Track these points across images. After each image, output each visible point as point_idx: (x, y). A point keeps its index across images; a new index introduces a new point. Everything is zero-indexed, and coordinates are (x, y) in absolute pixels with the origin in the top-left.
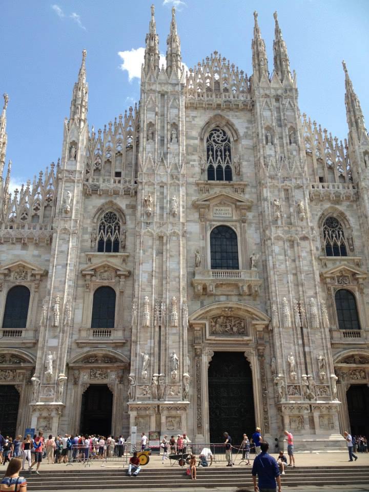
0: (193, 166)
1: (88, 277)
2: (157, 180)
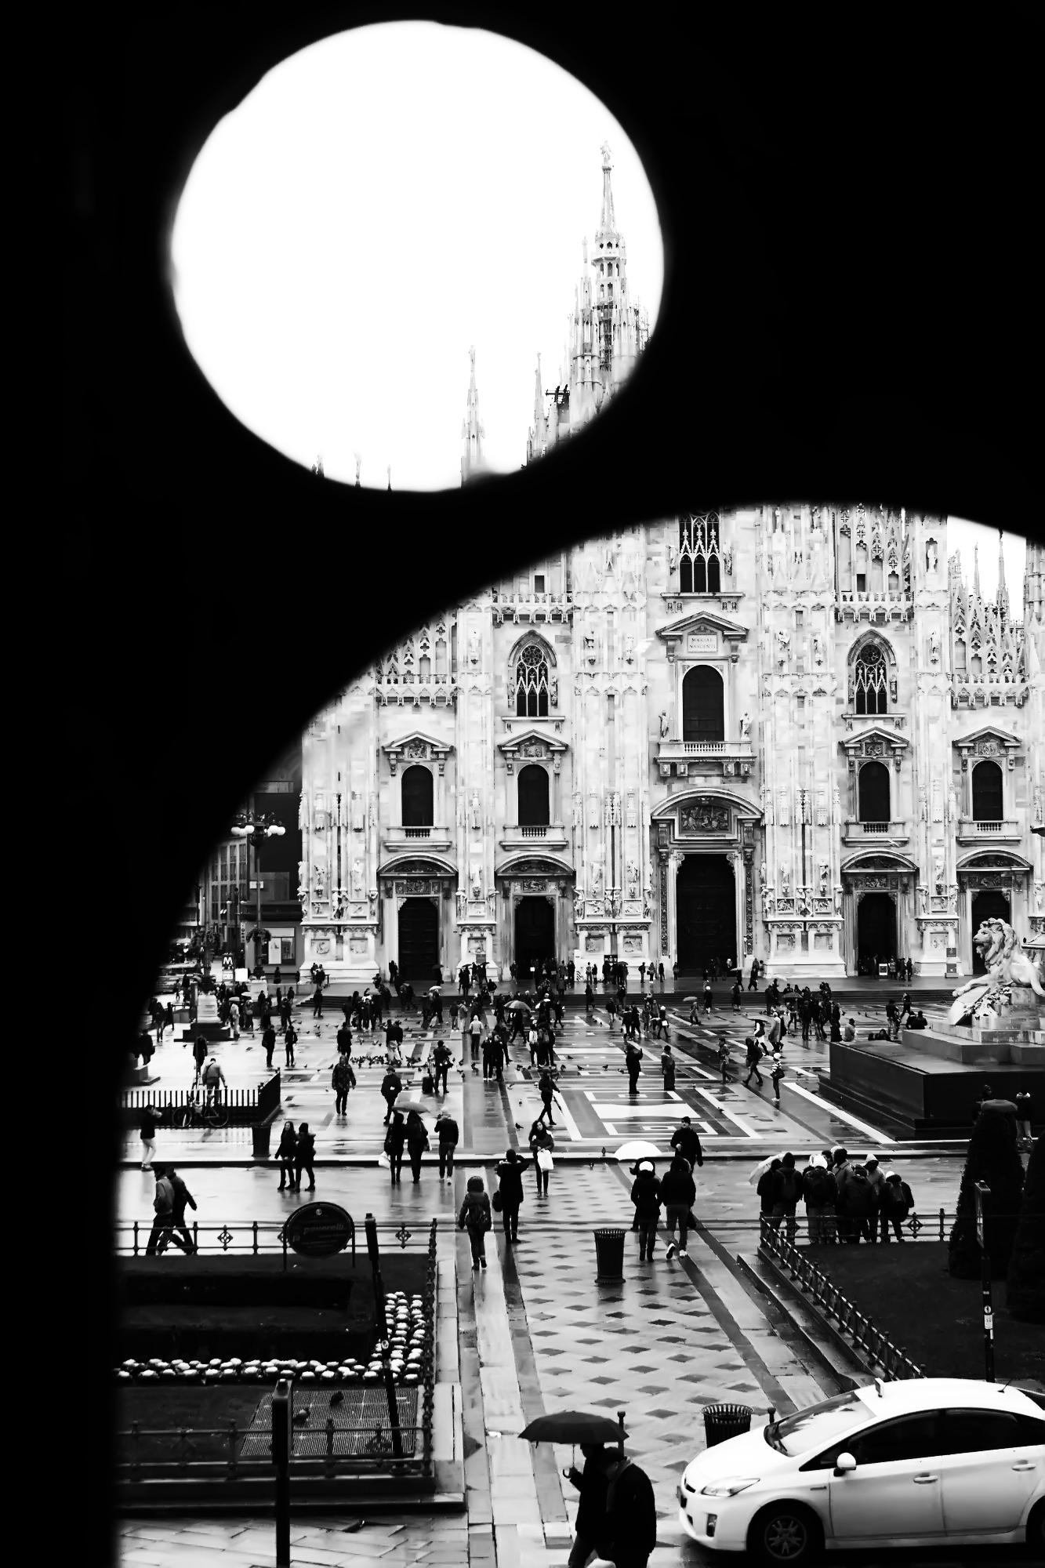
0: (656, 563)
1: (509, 755)
2: (602, 602)
